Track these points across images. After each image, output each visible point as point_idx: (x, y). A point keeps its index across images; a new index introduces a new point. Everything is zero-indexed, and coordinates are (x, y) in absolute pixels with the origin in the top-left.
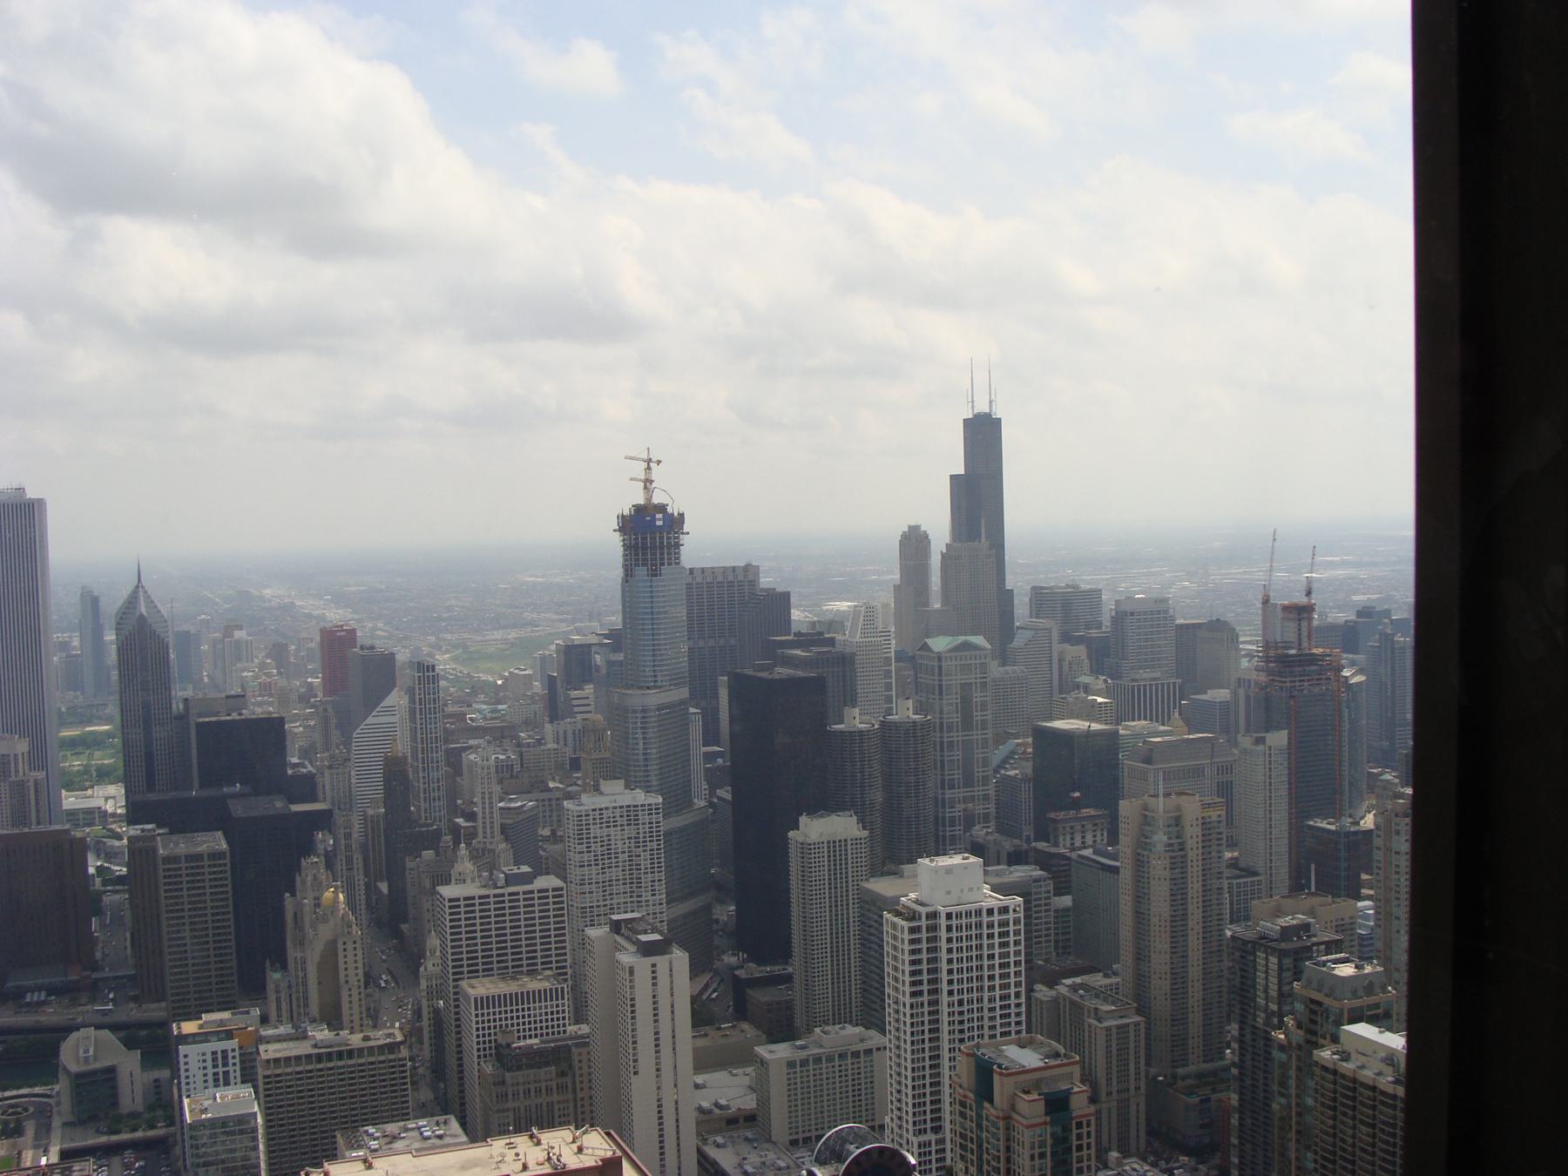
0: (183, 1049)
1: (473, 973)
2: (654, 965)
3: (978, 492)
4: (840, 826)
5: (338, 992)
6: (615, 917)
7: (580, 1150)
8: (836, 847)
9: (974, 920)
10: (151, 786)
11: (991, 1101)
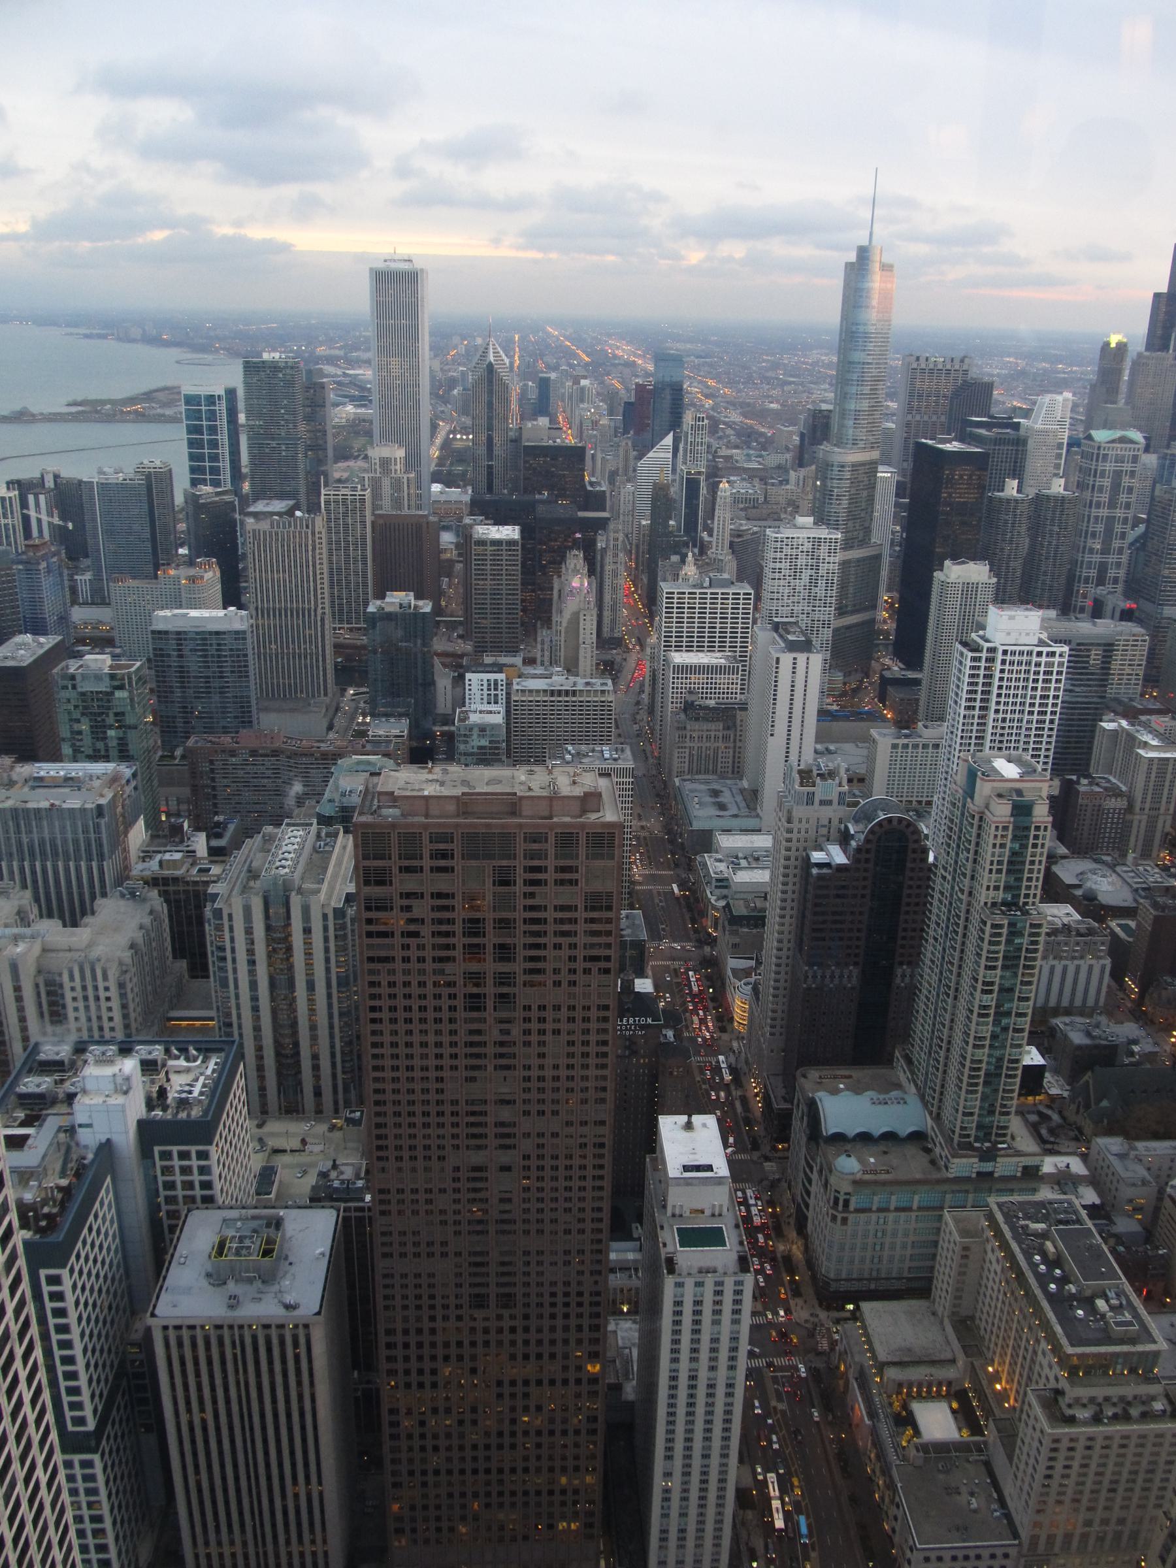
0: (468, 676)
1: (679, 648)
4: (977, 572)
5: (577, 649)
7: (574, 783)
8: (969, 589)
10: (490, 488)
11: (972, 798)
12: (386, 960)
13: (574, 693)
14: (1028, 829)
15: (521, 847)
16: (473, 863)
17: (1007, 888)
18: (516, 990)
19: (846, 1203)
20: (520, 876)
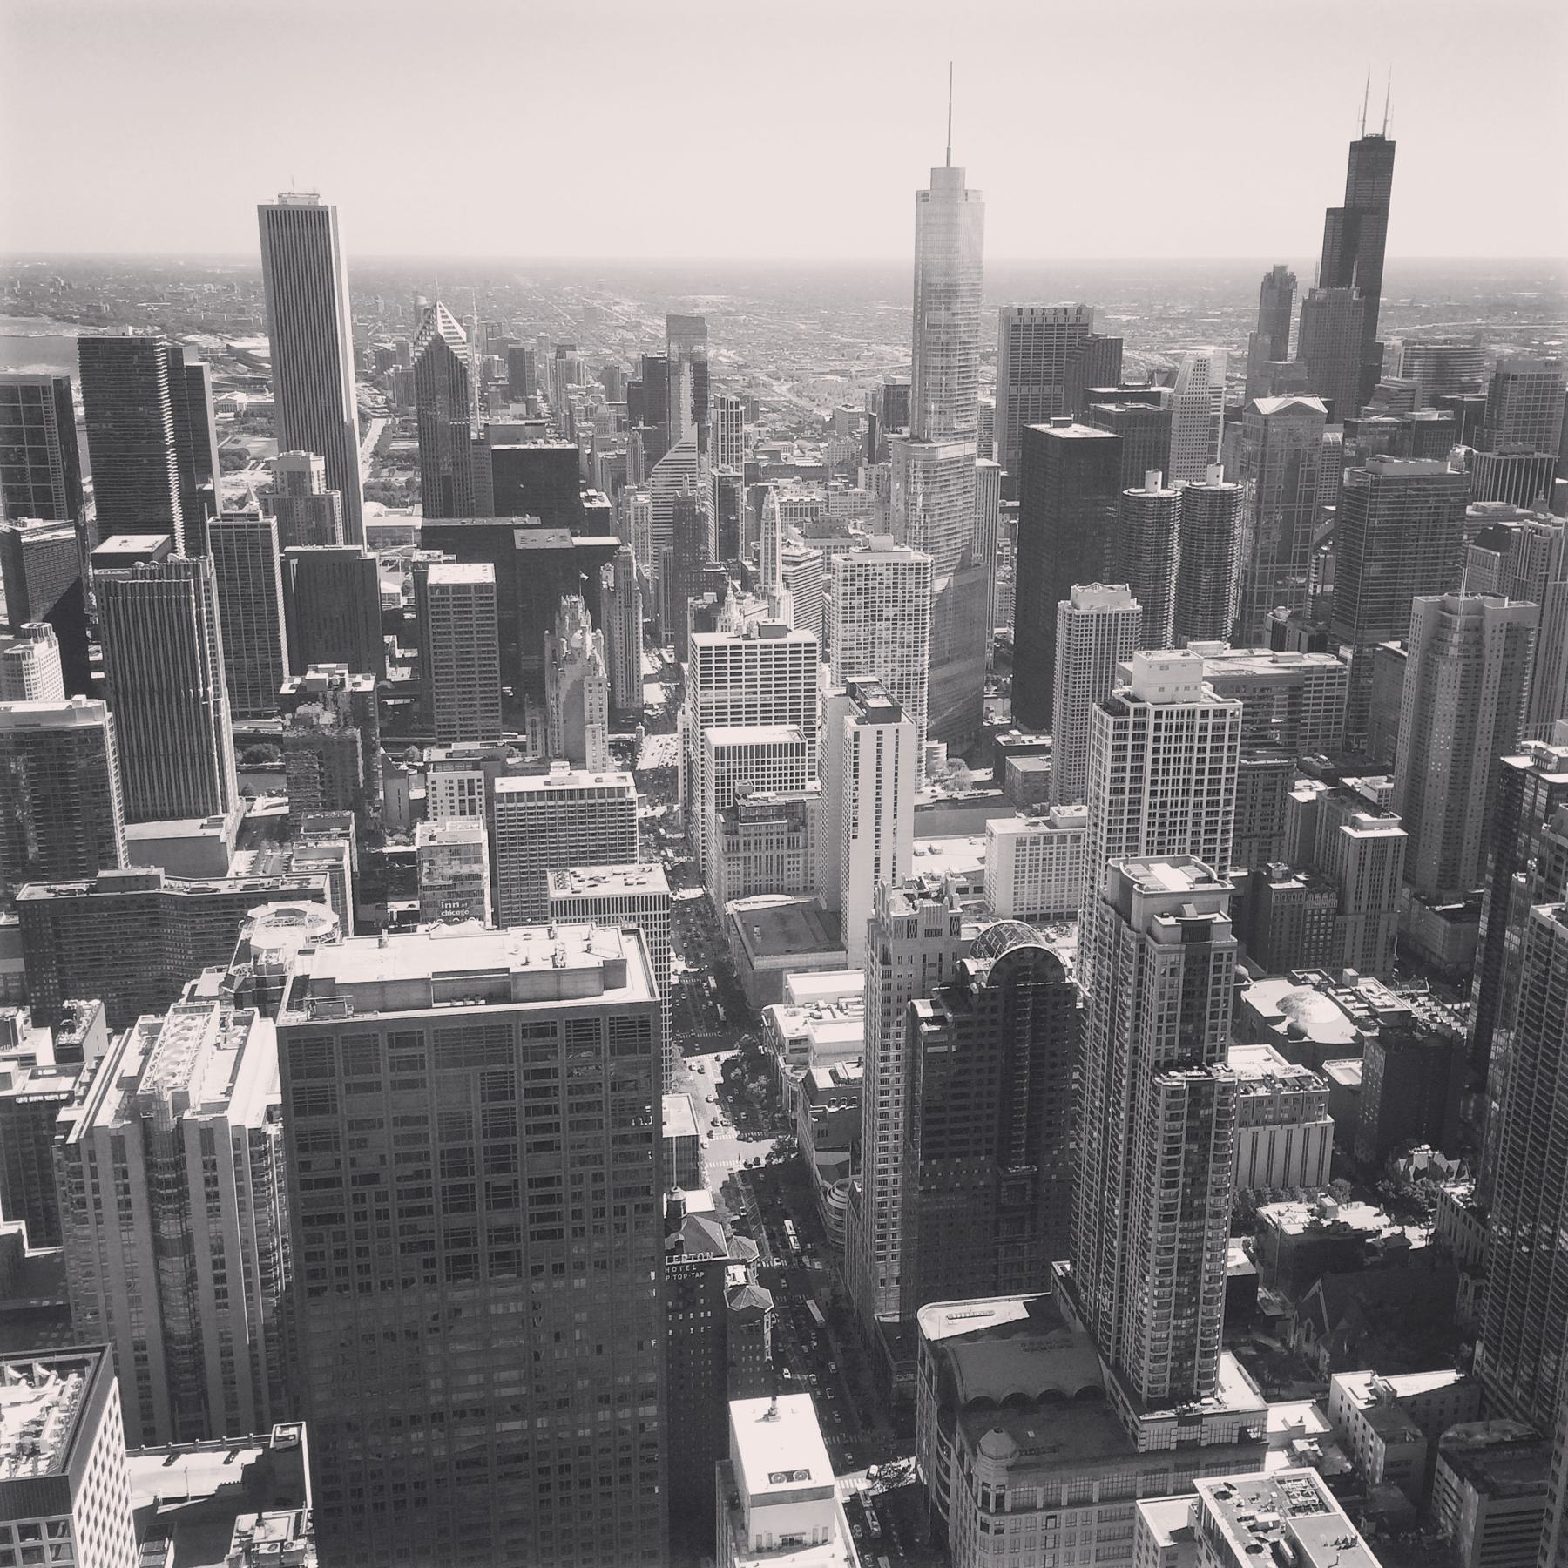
1: (721, 722)
2: (880, 732)
3: (1357, 230)
6: (851, 680)
7: (589, 950)
8: (1105, 622)
9: (1185, 720)
11: (1128, 921)
12: (331, 1219)
13: (581, 793)
14: (1206, 959)
15: (519, 1044)
16: (452, 1071)
17: (1184, 1041)
18: (521, 1246)
19: (1000, 1499)
20: (520, 1084)
